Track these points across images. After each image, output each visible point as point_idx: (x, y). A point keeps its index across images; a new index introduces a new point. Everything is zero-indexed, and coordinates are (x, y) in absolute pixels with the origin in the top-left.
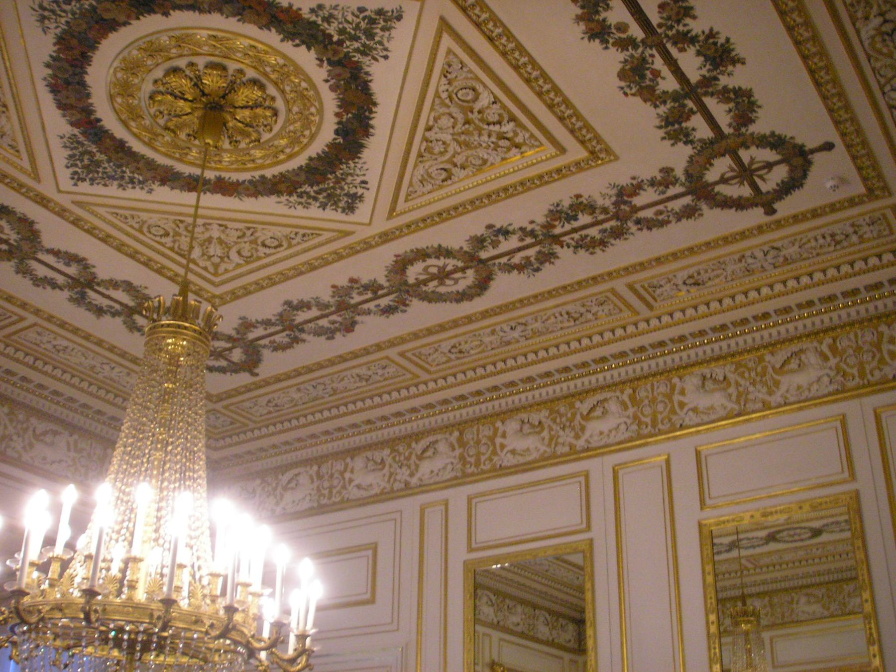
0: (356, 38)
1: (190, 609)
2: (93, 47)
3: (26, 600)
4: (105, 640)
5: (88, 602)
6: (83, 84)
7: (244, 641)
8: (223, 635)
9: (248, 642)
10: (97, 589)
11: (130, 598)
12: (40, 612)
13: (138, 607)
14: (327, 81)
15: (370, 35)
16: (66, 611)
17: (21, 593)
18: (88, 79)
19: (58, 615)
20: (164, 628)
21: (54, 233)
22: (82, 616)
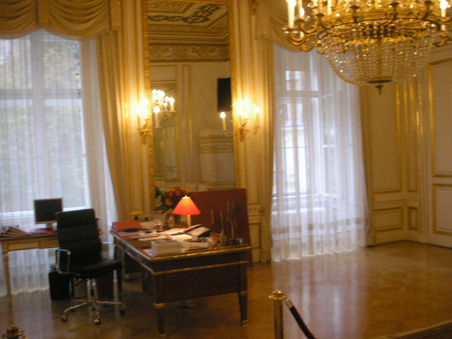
1: (404, 8)
3: (323, 19)
4: (364, 34)
5: (354, 12)
7: (435, 20)
8: (424, 19)
9: (439, 20)
10: (357, 5)
11: (374, 8)
12: (331, 23)
13: (378, 12)
16: (343, 21)
17: (320, 15)
19: (339, 23)
20: (395, 19)
22: (352, 21)
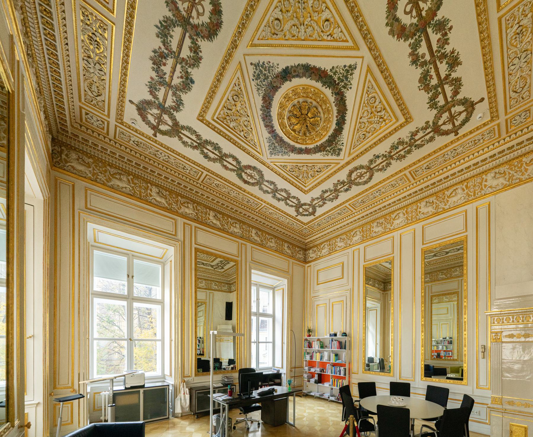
0: (342, 81)
2: (272, 100)
6: (270, 116)
14: (334, 102)
15: (347, 78)
18: (272, 113)
21: (268, 175)
